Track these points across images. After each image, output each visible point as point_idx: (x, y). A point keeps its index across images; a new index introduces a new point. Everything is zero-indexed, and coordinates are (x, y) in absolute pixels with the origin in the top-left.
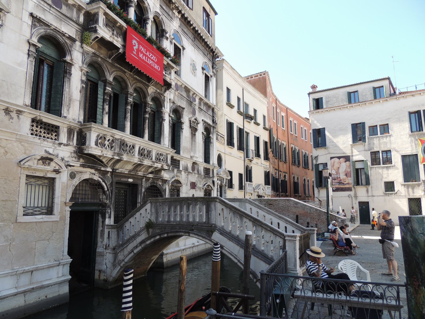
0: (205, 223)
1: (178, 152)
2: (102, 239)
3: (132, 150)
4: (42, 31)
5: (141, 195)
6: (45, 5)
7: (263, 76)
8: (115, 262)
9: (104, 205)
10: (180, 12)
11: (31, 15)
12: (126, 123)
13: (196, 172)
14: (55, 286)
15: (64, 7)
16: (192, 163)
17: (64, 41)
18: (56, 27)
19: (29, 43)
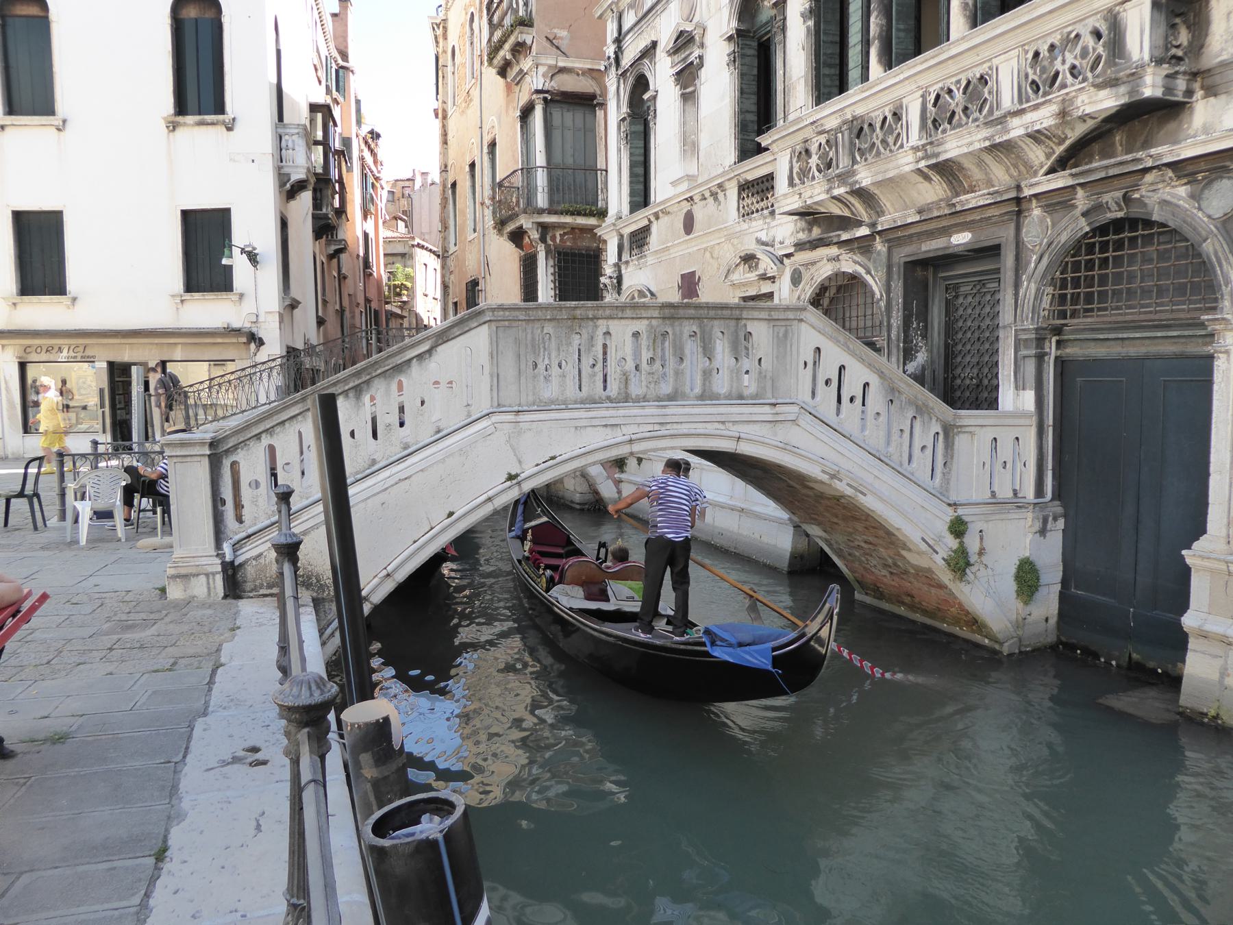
3: (892, 133)
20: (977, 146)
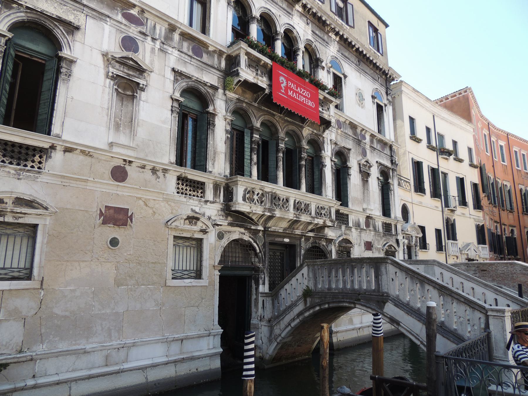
0: (374, 291)
1: (345, 204)
4: (183, 84)
5: (300, 258)
6: (186, 57)
7: (463, 94)
8: (271, 337)
9: (257, 270)
10: (337, 34)
11: (173, 70)
12: (278, 173)
13: (371, 228)
14: (206, 358)
15: (205, 55)
16: (365, 217)
17: (206, 91)
18: (198, 78)
19: (172, 99)
20: (308, 221)
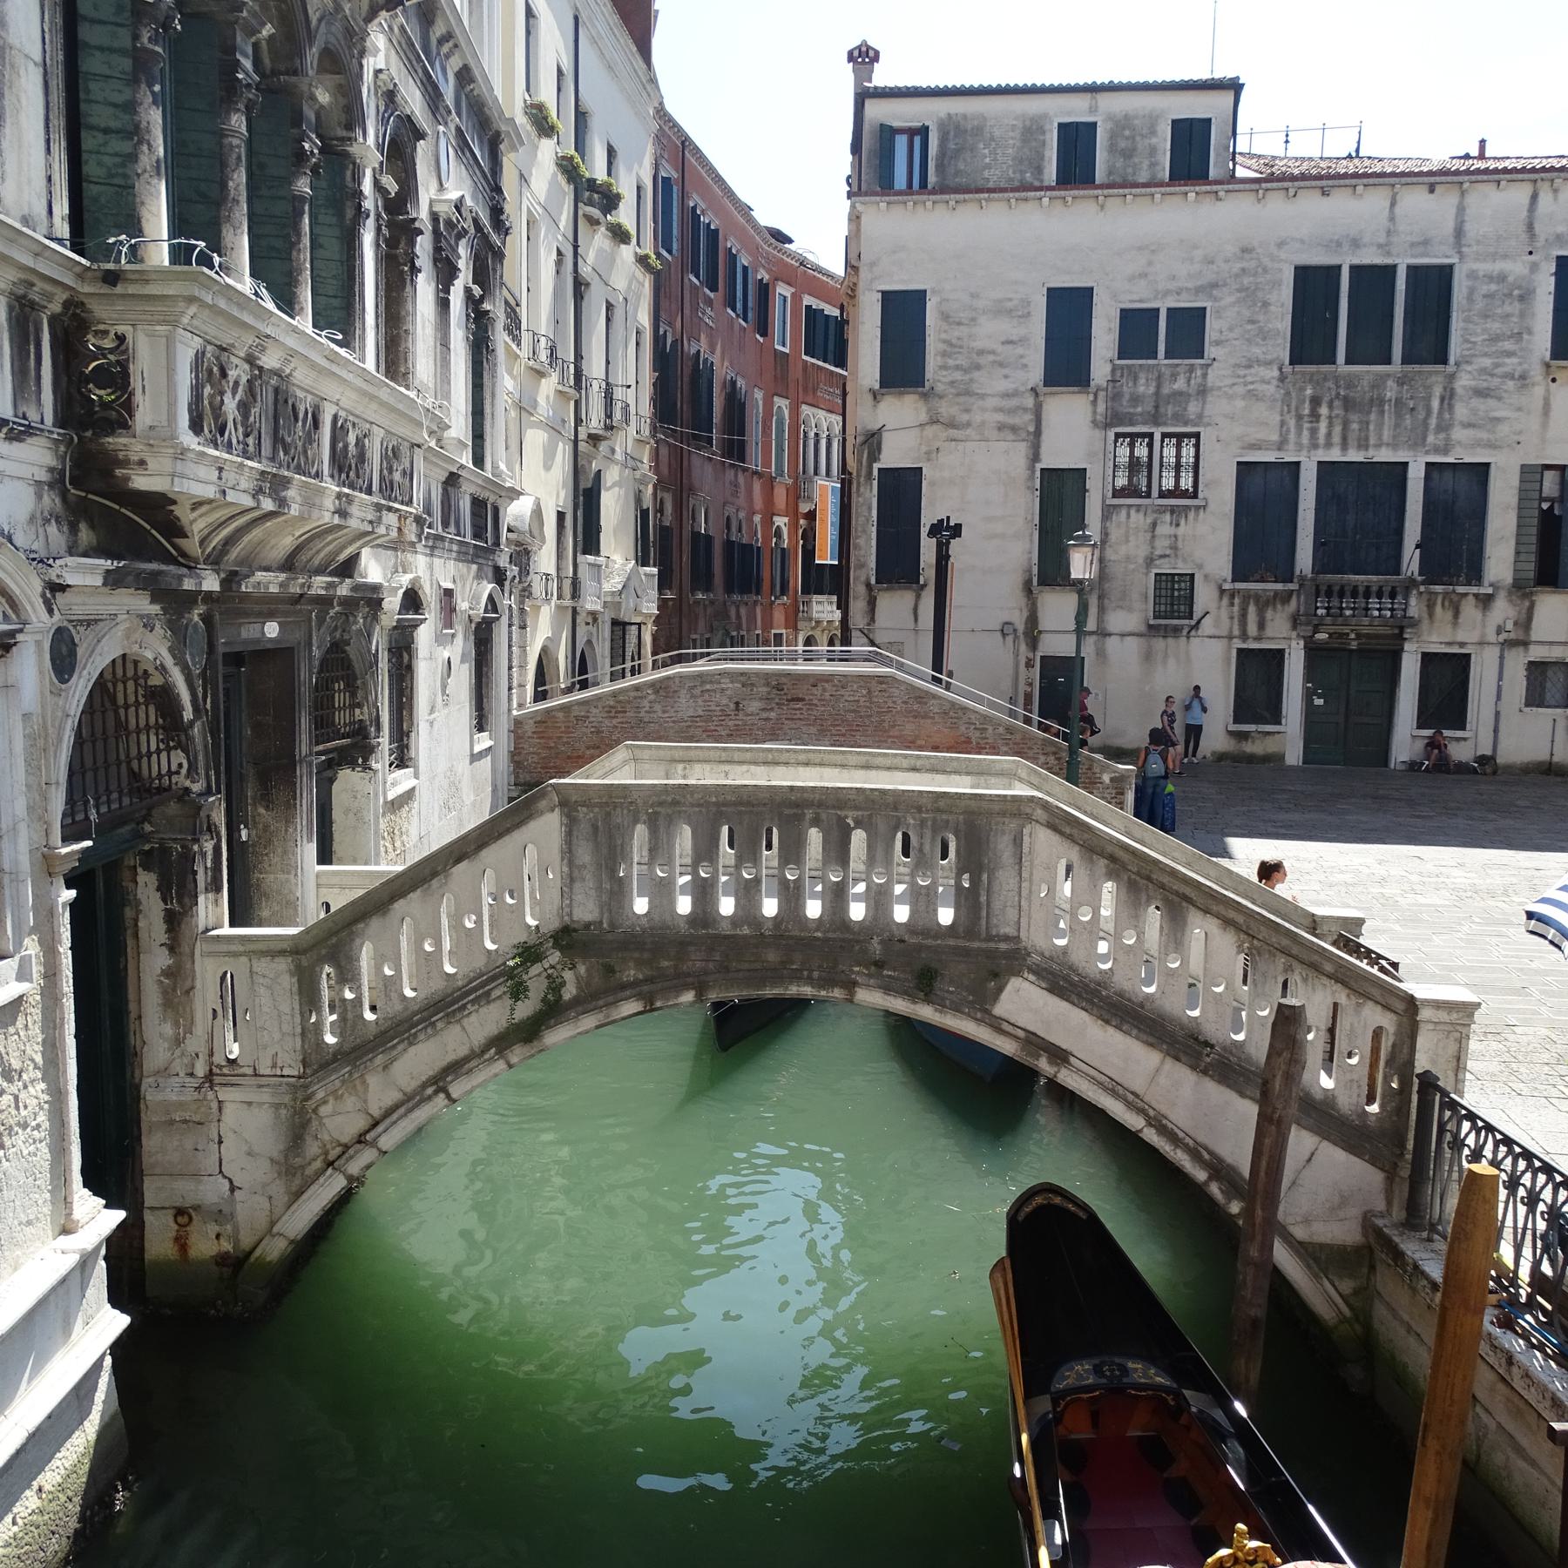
2: (177, 1024)
16: (443, 476)
